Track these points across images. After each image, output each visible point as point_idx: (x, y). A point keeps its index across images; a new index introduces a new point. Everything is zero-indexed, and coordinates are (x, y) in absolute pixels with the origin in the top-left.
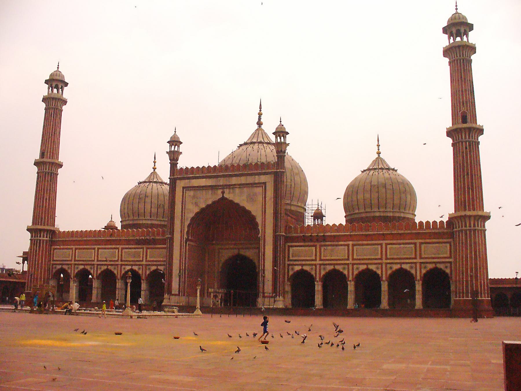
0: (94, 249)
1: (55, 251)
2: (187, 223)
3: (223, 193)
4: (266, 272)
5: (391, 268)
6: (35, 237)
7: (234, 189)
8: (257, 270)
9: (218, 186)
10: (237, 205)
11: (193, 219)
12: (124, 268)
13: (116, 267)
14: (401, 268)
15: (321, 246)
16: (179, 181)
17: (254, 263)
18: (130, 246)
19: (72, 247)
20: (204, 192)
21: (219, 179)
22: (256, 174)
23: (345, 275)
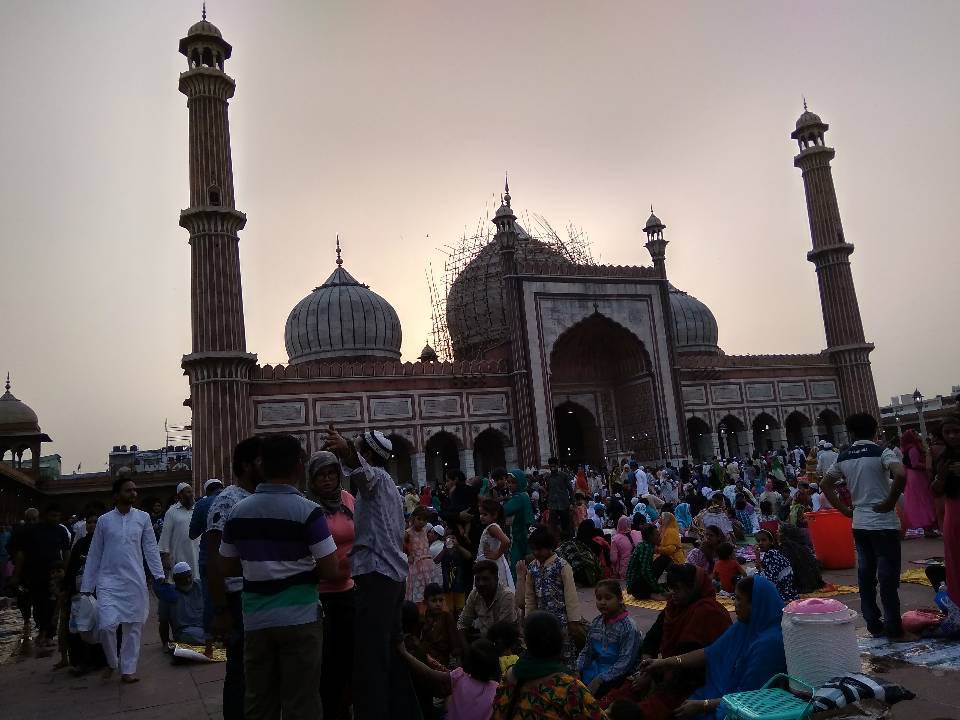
0: (360, 399)
2: (549, 350)
3: (596, 306)
4: (670, 423)
5: (786, 411)
6: (223, 376)
8: (597, 424)
9: (587, 295)
10: (618, 325)
11: (557, 345)
13: (412, 430)
14: (796, 412)
17: (590, 415)
19: (306, 396)
22: (636, 283)
23: (741, 423)
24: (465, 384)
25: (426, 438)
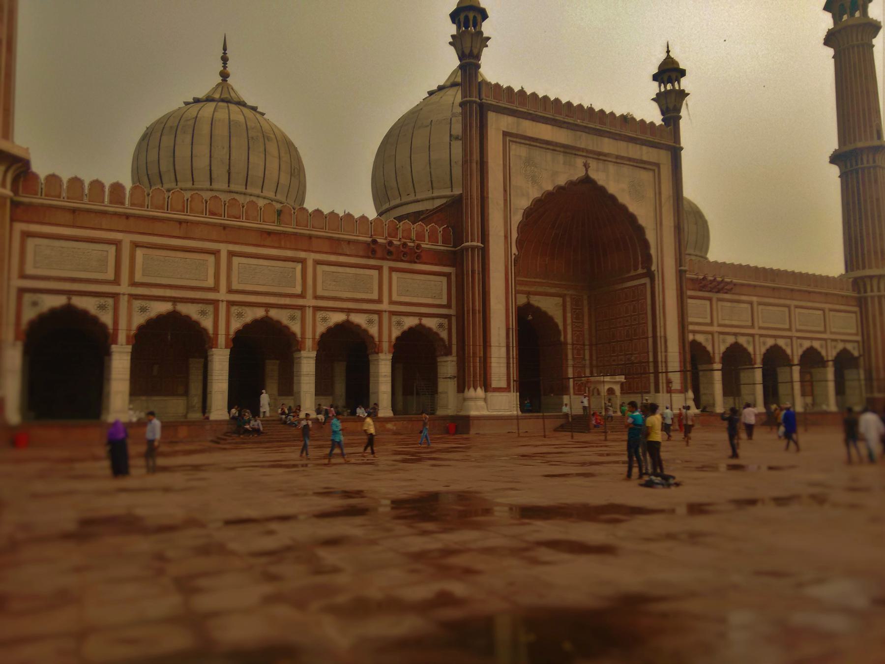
0: (216, 253)
1: (31, 243)
2: (517, 218)
3: (586, 166)
4: (669, 344)
7: (606, 162)
8: (562, 338)
9: (579, 149)
10: (613, 198)
12: (324, 319)
13: (298, 313)
15: (719, 300)
16: (494, 113)
17: (556, 325)
18: (342, 259)
19: (118, 236)
20: (549, 156)
21: (579, 133)
24: (390, 253)
25: (321, 329)
